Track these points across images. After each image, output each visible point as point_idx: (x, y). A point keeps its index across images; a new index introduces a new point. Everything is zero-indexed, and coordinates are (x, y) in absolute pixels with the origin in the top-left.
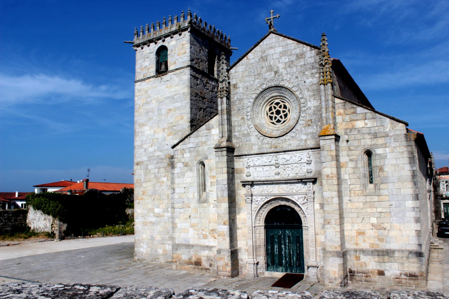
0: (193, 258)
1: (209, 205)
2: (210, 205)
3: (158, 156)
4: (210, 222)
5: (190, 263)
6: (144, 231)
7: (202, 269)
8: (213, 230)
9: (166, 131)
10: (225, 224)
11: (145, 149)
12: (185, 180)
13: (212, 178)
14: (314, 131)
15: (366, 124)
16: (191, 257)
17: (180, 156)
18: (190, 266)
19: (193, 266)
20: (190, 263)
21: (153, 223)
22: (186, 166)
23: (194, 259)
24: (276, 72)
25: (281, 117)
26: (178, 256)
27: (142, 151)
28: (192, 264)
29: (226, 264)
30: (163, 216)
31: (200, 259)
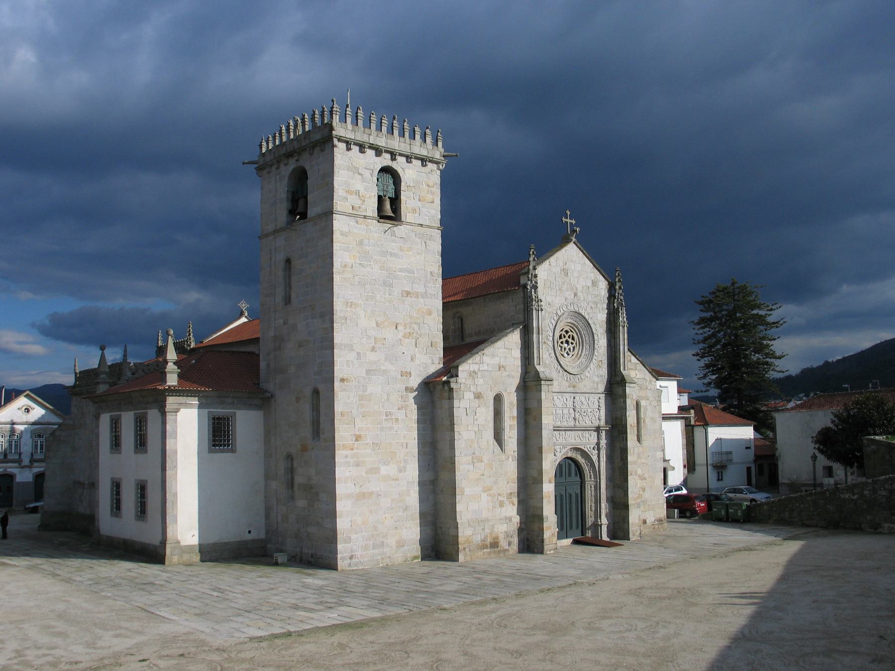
0: (488, 538)
1: (507, 457)
2: (508, 458)
4: (508, 483)
5: (484, 547)
7: (499, 552)
9: (400, 328)
10: (550, 482)
12: (477, 419)
13: (511, 419)
14: (604, 374)
15: (636, 375)
16: (486, 537)
18: (485, 550)
19: (488, 550)
20: (484, 547)
22: (478, 398)
23: (489, 540)
24: (575, 295)
25: (569, 349)
26: (468, 539)
27: (352, 356)
28: (487, 547)
29: (552, 534)
31: (497, 538)
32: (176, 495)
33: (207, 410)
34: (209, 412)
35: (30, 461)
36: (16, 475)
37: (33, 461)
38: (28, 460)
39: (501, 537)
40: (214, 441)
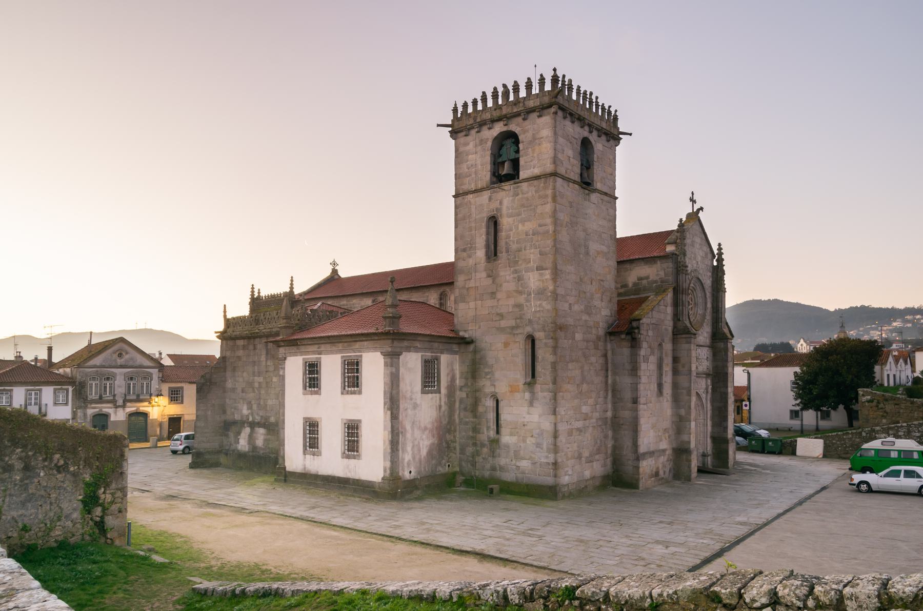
3: (586, 321)
6: (568, 446)
8: (665, 429)
11: (570, 304)
17: (645, 333)
18: (653, 479)
21: (579, 430)
30: (591, 418)
32: (385, 429)
33: (420, 354)
34: (422, 356)
35: (124, 402)
36: (110, 414)
37: (125, 401)
38: (122, 401)
39: (660, 466)
40: (425, 382)
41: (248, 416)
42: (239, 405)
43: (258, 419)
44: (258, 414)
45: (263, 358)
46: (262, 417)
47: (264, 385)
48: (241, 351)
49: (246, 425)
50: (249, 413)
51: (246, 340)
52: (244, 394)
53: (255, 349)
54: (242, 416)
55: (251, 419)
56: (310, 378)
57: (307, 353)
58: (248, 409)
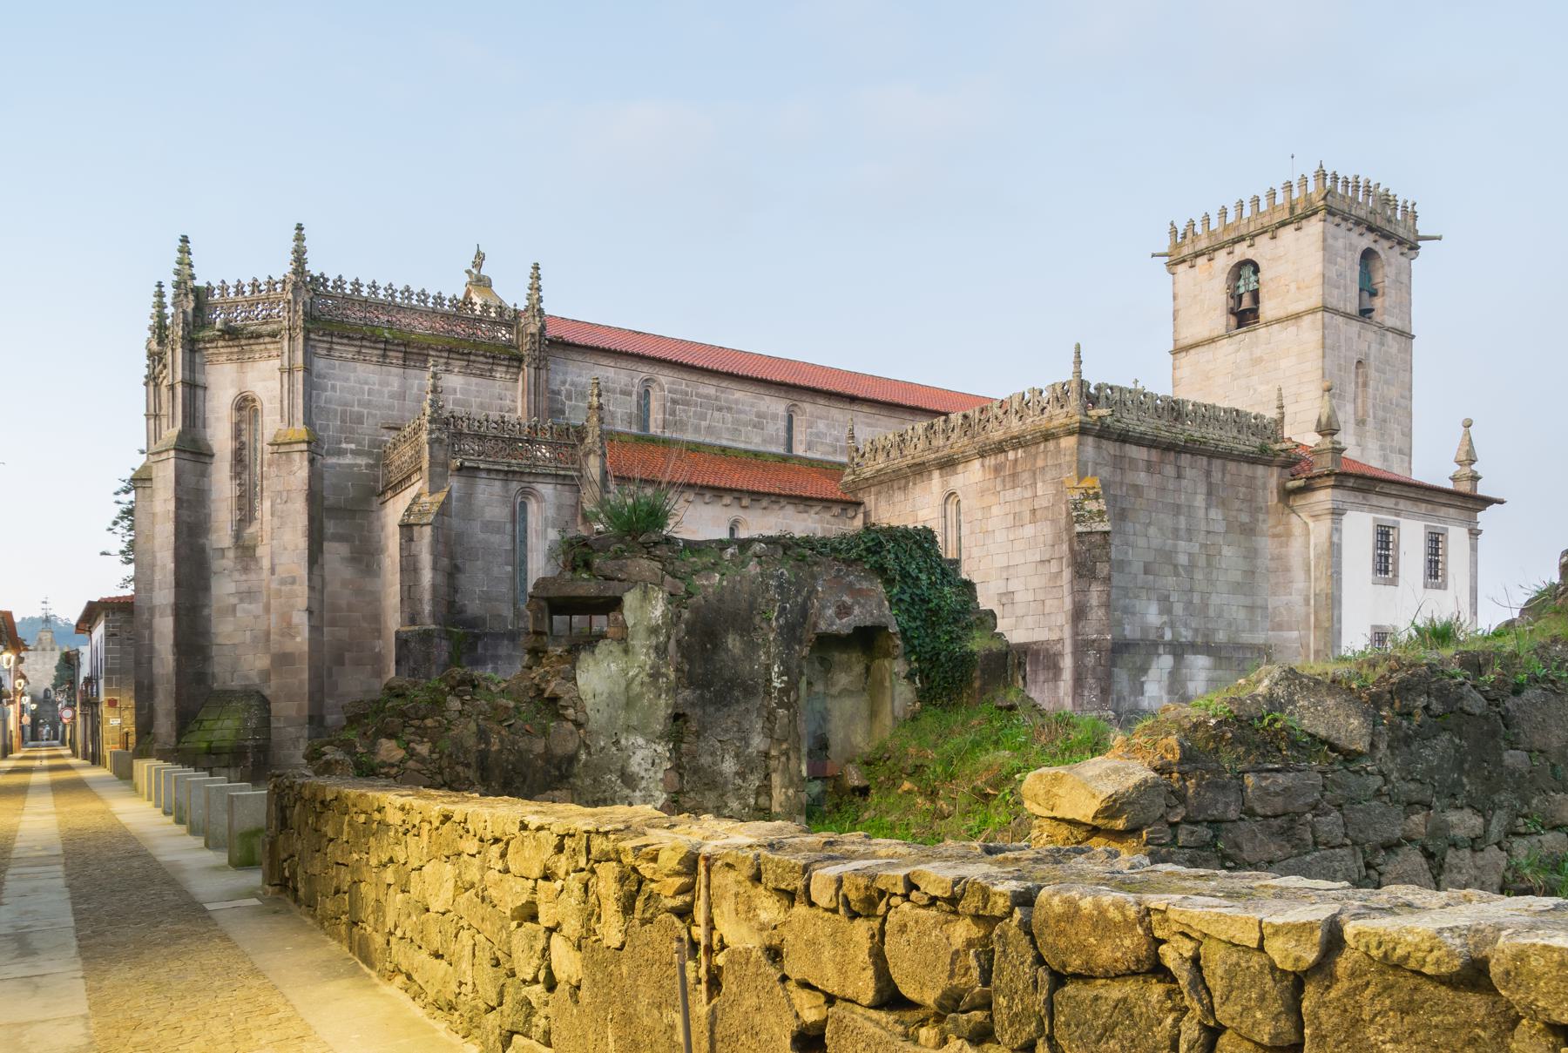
41: (1161, 628)
42: (1137, 603)
43: (1186, 635)
44: (1186, 625)
45: (1200, 501)
46: (1196, 630)
47: (1202, 561)
48: (1143, 475)
49: (1161, 650)
50: (1165, 623)
51: (1154, 452)
52: (1151, 577)
53: (1179, 477)
54: (1145, 629)
55: (1168, 636)
56: (1380, 555)
57: (1380, 508)
58: (1161, 613)
